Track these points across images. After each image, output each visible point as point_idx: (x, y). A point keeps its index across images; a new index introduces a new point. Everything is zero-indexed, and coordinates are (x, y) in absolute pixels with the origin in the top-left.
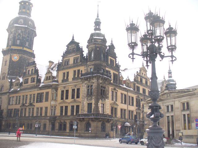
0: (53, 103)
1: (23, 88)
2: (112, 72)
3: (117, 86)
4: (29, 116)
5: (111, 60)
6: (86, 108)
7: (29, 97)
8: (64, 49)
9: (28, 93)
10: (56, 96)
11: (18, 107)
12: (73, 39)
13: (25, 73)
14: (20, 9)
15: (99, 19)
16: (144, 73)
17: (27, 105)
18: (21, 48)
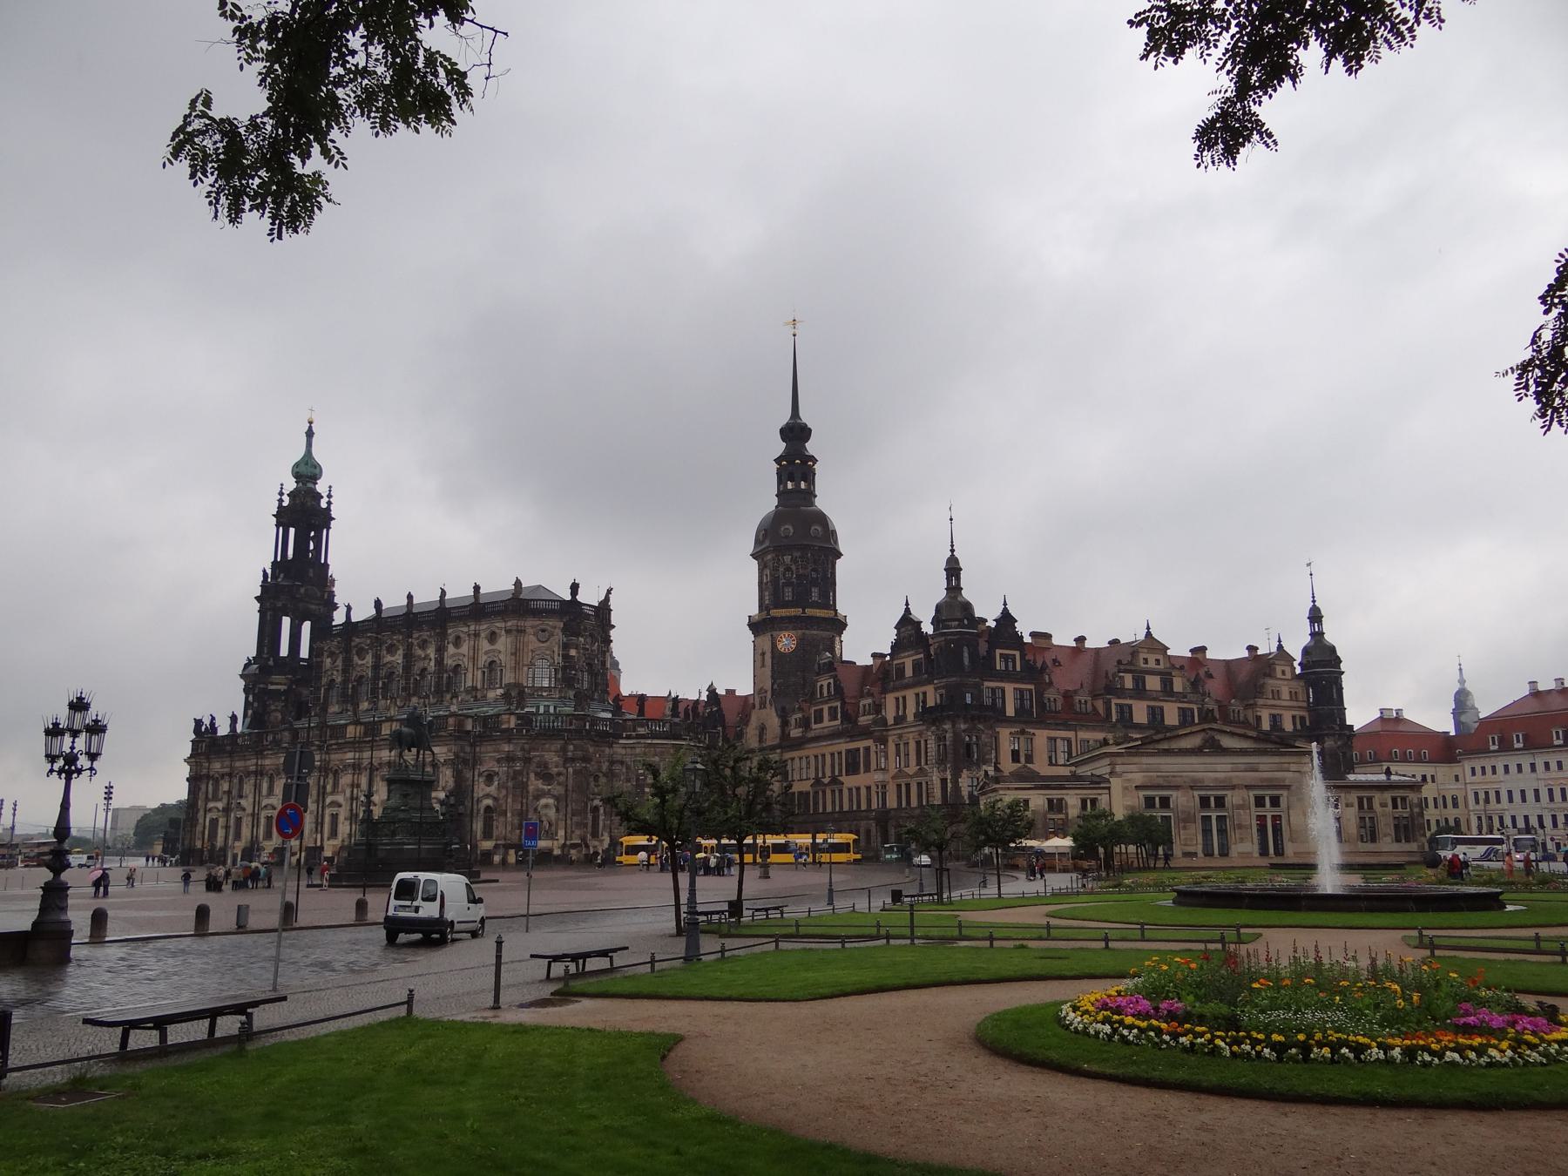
0: (878, 777)
1: (810, 734)
2: (1009, 688)
3: (1025, 722)
4: (833, 812)
5: (1005, 657)
6: (938, 792)
7: (828, 758)
8: (892, 635)
9: (827, 748)
10: (887, 758)
11: (805, 786)
12: (907, 610)
13: (813, 693)
14: (780, 481)
15: (957, 561)
16: (1152, 658)
17: (826, 780)
18: (797, 611)
